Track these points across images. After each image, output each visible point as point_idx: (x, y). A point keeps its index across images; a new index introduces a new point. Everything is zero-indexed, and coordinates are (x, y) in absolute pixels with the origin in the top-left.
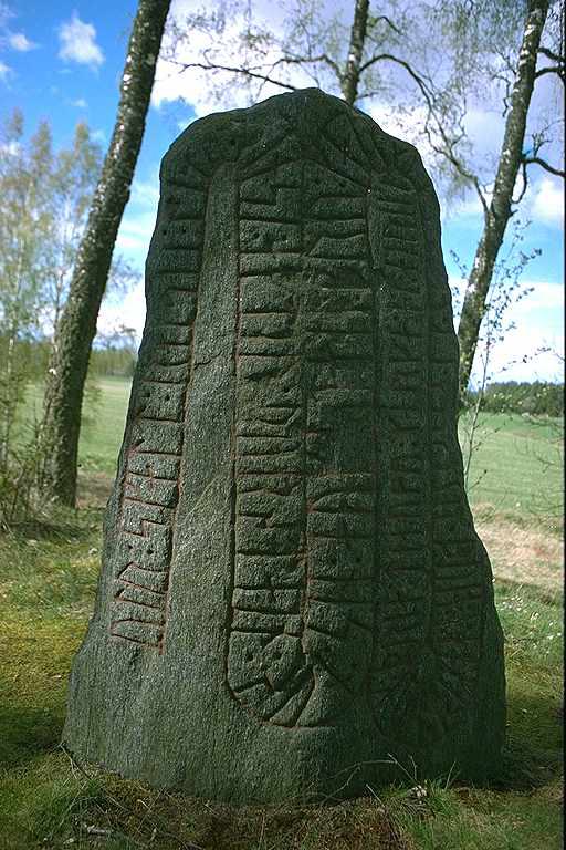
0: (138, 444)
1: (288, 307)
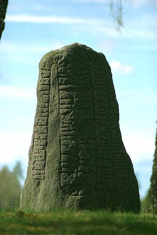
0: (37, 132)
1: (71, 97)
